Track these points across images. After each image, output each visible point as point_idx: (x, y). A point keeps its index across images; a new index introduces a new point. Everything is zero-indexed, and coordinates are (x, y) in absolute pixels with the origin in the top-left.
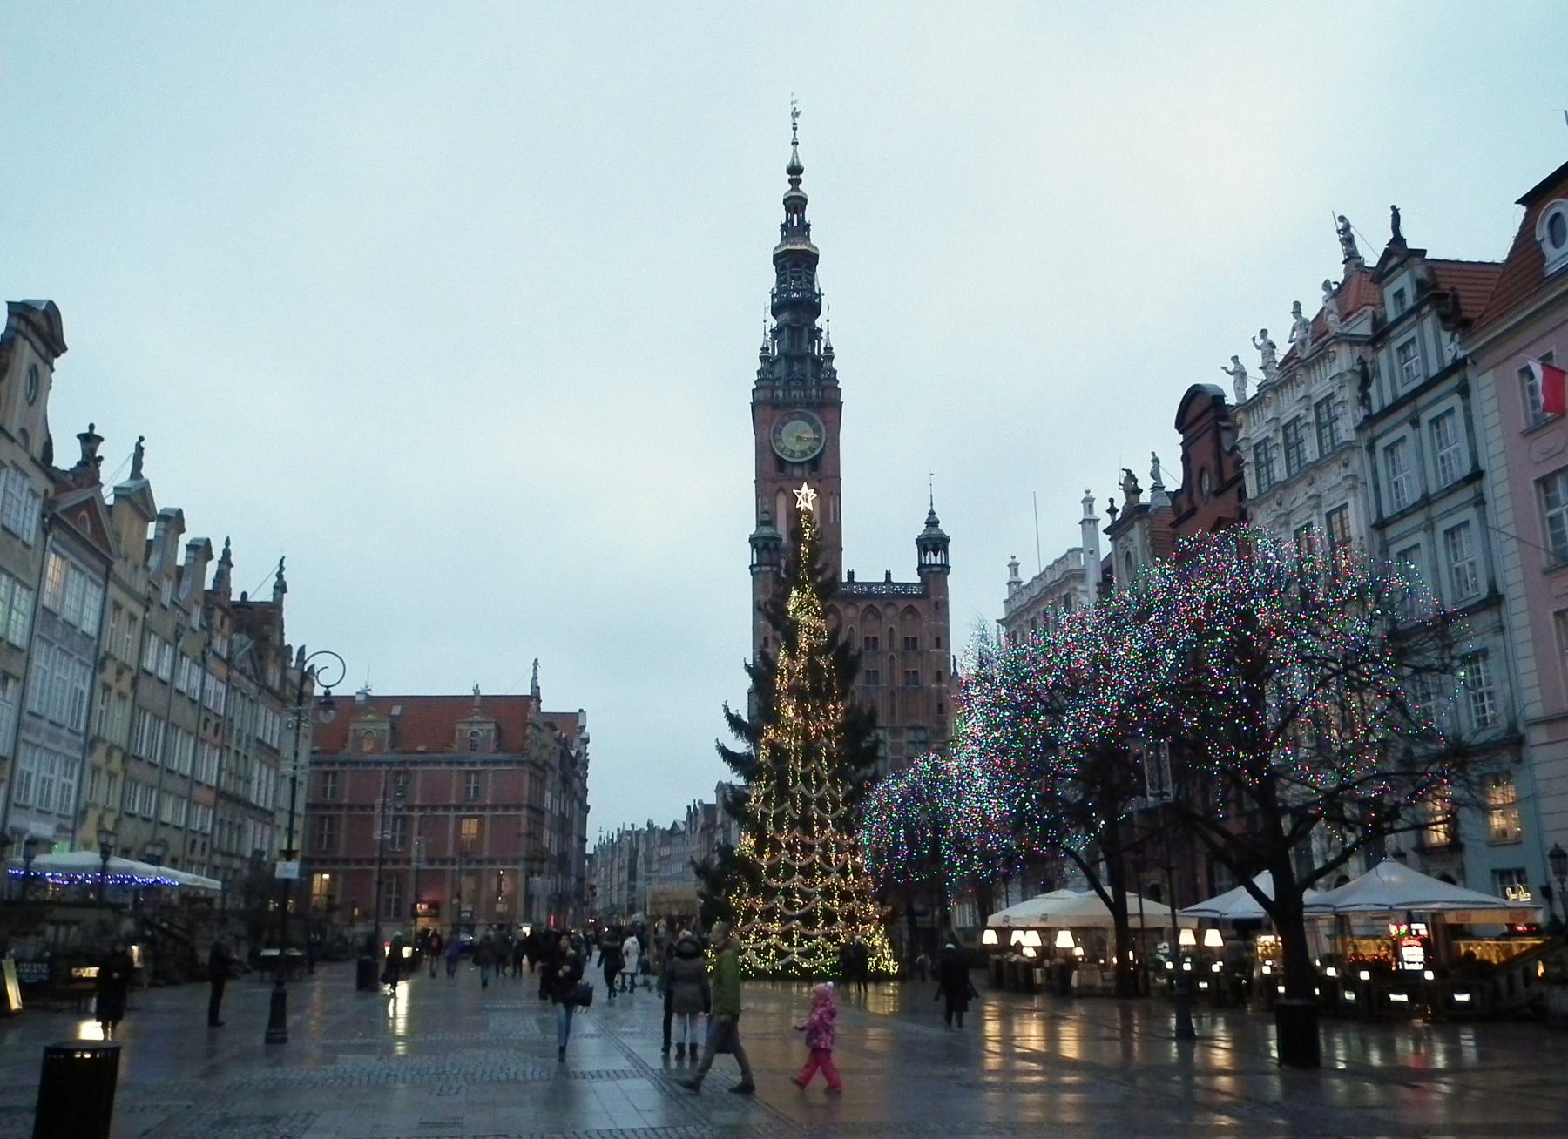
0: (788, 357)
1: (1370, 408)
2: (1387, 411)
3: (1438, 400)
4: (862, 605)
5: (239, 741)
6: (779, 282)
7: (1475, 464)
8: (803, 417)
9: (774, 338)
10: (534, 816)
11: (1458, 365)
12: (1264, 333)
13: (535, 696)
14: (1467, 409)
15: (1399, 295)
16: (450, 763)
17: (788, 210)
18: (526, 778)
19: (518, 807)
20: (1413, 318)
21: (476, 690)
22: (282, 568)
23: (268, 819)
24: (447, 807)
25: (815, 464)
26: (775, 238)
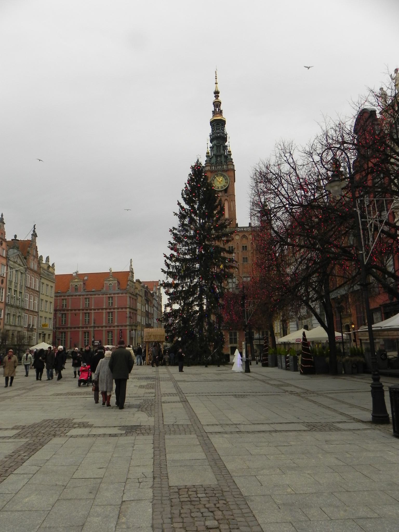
0: (217, 156)
4: (241, 234)
5: (16, 287)
6: (213, 131)
8: (222, 175)
9: (211, 151)
10: (132, 311)
13: (132, 272)
16: (103, 294)
17: (215, 106)
18: (128, 299)
19: (126, 308)
21: (110, 270)
22: (35, 229)
23: (36, 314)
24: (102, 309)
25: (226, 191)
26: (210, 117)
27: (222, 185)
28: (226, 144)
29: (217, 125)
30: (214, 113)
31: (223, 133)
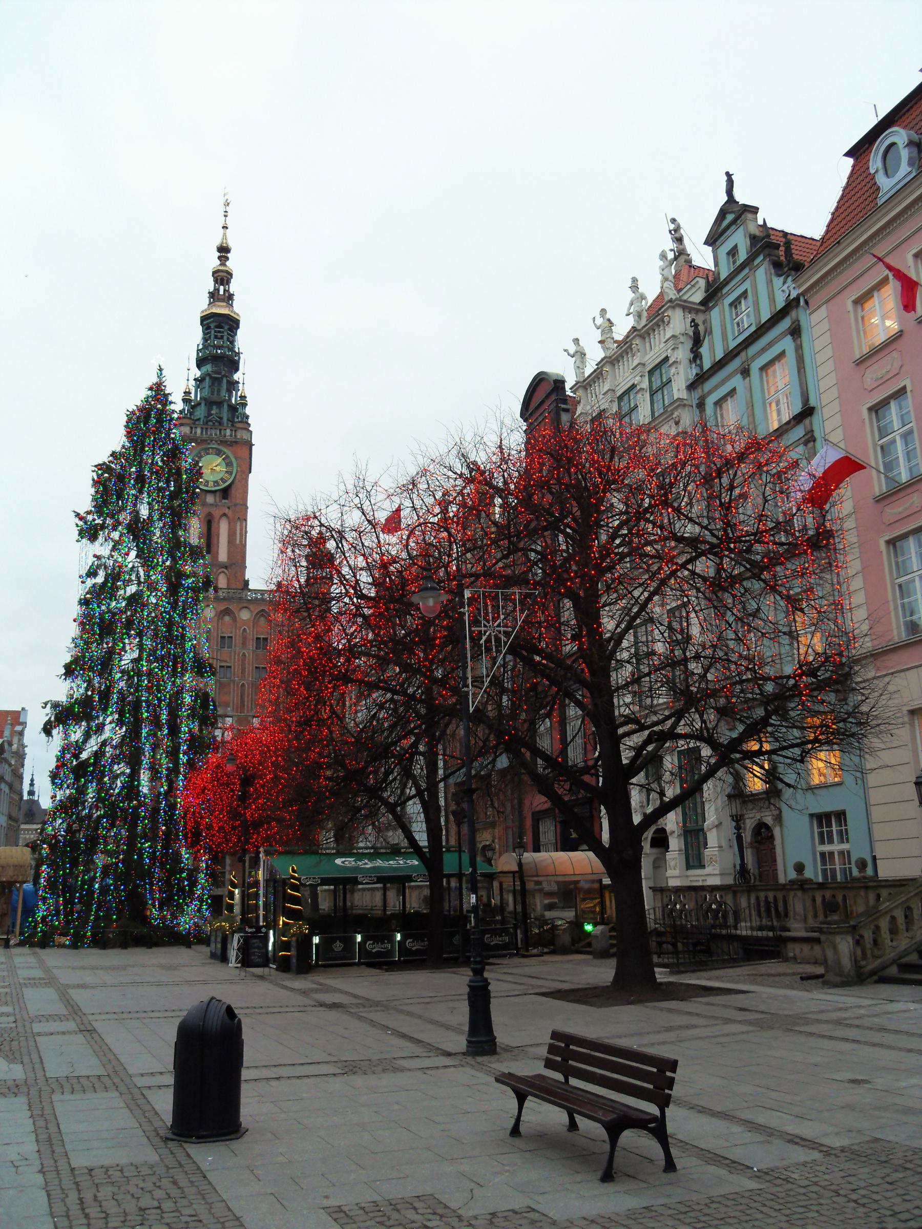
0: (209, 403)
1: (701, 367)
2: (719, 365)
3: (770, 345)
4: (257, 609)
6: (205, 339)
7: (805, 398)
8: (219, 453)
9: (197, 387)
11: (792, 305)
12: (603, 312)
14: (799, 349)
15: (733, 252)
17: (216, 281)
20: (746, 271)
25: (225, 493)
26: (202, 304)
27: (217, 477)
28: (236, 377)
29: (216, 327)
30: (213, 295)
31: (232, 349)
